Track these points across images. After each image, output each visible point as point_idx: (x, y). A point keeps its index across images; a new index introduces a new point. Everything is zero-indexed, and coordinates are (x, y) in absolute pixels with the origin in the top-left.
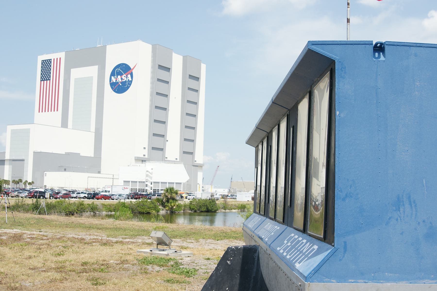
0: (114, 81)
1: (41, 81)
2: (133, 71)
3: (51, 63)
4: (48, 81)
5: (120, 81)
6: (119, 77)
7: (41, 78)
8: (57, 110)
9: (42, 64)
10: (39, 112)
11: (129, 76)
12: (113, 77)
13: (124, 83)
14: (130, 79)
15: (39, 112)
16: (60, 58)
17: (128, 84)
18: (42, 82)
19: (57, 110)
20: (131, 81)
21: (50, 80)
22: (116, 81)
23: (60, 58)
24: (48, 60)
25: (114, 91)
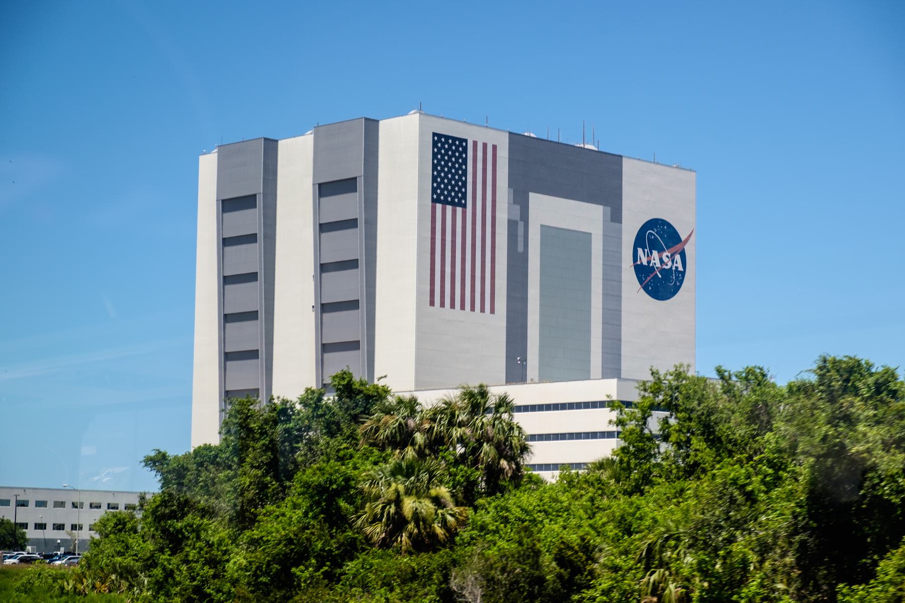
0: (645, 263)
1: (434, 201)
2: (686, 247)
3: (465, 150)
4: (459, 210)
5: (658, 265)
6: (655, 253)
7: (434, 190)
8: (492, 311)
9: (435, 144)
10: (432, 303)
11: (678, 257)
12: (640, 250)
13: (666, 273)
14: (681, 269)
15: (432, 303)
16: (495, 147)
17: (677, 277)
18: (439, 206)
19: (492, 311)
20: (683, 273)
21: (464, 206)
22: (649, 262)
23: (495, 147)
24: (454, 139)
25: (645, 288)
